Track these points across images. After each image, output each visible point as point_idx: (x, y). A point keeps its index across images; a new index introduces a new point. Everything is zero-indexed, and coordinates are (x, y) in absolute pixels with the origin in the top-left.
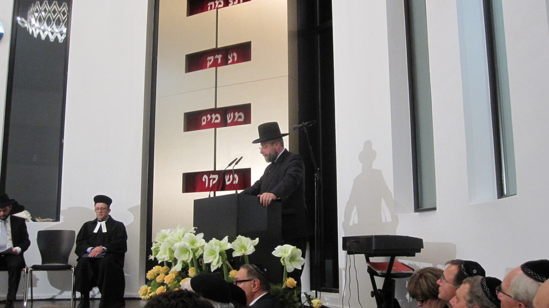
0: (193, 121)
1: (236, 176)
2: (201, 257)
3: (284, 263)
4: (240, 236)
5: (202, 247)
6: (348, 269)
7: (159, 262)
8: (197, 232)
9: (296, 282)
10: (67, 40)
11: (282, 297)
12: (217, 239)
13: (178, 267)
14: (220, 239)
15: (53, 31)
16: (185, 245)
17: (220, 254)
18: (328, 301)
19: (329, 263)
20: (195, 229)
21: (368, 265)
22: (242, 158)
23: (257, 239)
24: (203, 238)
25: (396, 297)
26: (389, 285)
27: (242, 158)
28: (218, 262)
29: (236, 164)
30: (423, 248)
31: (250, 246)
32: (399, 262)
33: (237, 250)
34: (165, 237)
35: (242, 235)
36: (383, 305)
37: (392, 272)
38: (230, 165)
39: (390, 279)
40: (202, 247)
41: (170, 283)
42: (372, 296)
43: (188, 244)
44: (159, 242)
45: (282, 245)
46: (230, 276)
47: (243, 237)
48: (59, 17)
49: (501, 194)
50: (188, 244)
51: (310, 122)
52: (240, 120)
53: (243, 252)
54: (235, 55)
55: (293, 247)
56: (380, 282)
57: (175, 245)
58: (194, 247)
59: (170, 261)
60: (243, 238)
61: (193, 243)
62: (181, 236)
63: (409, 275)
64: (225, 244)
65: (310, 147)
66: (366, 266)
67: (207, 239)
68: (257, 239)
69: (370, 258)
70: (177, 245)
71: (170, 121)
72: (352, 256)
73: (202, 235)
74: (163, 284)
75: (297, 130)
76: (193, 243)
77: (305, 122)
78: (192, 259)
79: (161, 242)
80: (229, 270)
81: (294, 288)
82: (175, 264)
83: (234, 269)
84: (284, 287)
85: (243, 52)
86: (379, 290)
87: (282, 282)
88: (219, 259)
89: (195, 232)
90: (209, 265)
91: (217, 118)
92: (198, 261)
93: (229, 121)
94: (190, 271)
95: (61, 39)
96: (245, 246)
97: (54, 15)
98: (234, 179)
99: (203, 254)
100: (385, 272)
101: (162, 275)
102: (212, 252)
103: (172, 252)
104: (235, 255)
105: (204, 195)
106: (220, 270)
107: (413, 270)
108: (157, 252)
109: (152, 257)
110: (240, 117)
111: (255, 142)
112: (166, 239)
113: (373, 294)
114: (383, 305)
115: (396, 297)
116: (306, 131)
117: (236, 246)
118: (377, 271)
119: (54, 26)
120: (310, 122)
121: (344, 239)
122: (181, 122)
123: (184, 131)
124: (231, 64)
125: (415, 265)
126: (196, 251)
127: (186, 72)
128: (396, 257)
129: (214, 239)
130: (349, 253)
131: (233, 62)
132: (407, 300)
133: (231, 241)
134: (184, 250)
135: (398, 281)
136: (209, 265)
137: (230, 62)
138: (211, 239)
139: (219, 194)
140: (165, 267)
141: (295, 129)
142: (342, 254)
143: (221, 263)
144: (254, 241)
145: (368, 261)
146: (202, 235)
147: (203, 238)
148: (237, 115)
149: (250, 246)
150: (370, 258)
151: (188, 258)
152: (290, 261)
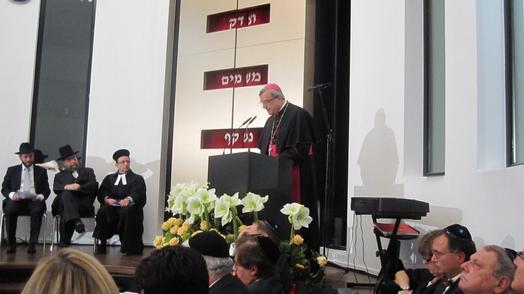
0: (213, 80)
1: (251, 134)
2: (213, 211)
3: (292, 221)
5: (214, 202)
6: (355, 228)
7: (174, 214)
8: (210, 187)
9: (303, 240)
11: (289, 253)
13: (191, 221)
14: (231, 195)
16: (197, 200)
18: (335, 258)
19: (338, 221)
20: (208, 185)
21: (375, 225)
22: (256, 117)
23: (267, 197)
24: (215, 194)
25: (401, 257)
26: (394, 246)
27: (256, 117)
28: (229, 217)
29: (250, 123)
30: (428, 212)
31: (260, 203)
32: (405, 224)
34: (180, 190)
35: (252, 192)
36: (388, 266)
37: (398, 234)
38: (244, 124)
39: (395, 240)
40: (214, 202)
41: (182, 235)
42: (377, 256)
43: (200, 199)
44: (174, 196)
45: (291, 203)
47: (253, 194)
49: (510, 162)
50: (200, 199)
51: (324, 84)
52: (256, 80)
53: (253, 208)
54: (254, 16)
55: (301, 206)
56: (385, 243)
57: (188, 199)
58: (206, 202)
59: (184, 214)
60: (253, 194)
61: (205, 198)
62: (194, 192)
63: (415, 237)
64: (235, 200)
65: (324, 109)
66: (372, 226)
67: (219, 194)
68: (267, 197)
69: (377, 220)
70: (190, 199)
71: (190, 79)
72: (359, 216)
73: (214, 190)
74: (176, 235)
75: (312, 92)
76: (205, 198)
77: (320, 84)
78: (204, 213)
79: (175, 196)
80: (239, 225)
81: (301, 245)
82: (189, 216)
83: (244, 224)
84: (291, 243)
85: (263, 13)
86: (385, 250)
87: (288, 239)
88: (229, 214)
89: (208, 187)
90: (220, 219)
92: (210, 216)
93: (247, 81)
94: (201, 225)
96: (255, 202)
98: (250, 137)
99: (214, 209)
100: (390, 233)
101: (176, 227)
102: (224, 207)
103: (185, 205)
104: (245, 210)
105: (218, 152)
106: (230, 224)
107: (419, 233)
108: (172, 204)
109: (168, 209)
110: (257, 77)
111: (17, 153)
112: (180, 193)
113: (378, 254)
114: (388, 266)
115: (400, 258)
116: (320, 93)
117: (246, 202)
118: (383, 233)
120: (324, 84)
121: (353, 199)
122: (201, 81)
123: (204, 90)
124: (250, 25)
125: (421, 227)
126: (208, 206)
127: (207, 32)
128: (402, 220)
129: (225, 195)
130: (357, 213)
131: (252, 24)
132: (412, 261)
133: (241, 197)
134: (197, 204)
135: (403, 243)
136: (220, 219)
137: (250, 23)
138: (223, 195)
139: (235, 151)
140: (180, 219)
141: (309, 90)
142: (350, 213)
143: (231, 218)
144: (264, 198)
145: (375, 221)
146: (214, 190)
147: (215, 194)
148: (254, 75)
149: (260, 203)
150: (377, 220)
151: (200, 212)
152: (298, 219)
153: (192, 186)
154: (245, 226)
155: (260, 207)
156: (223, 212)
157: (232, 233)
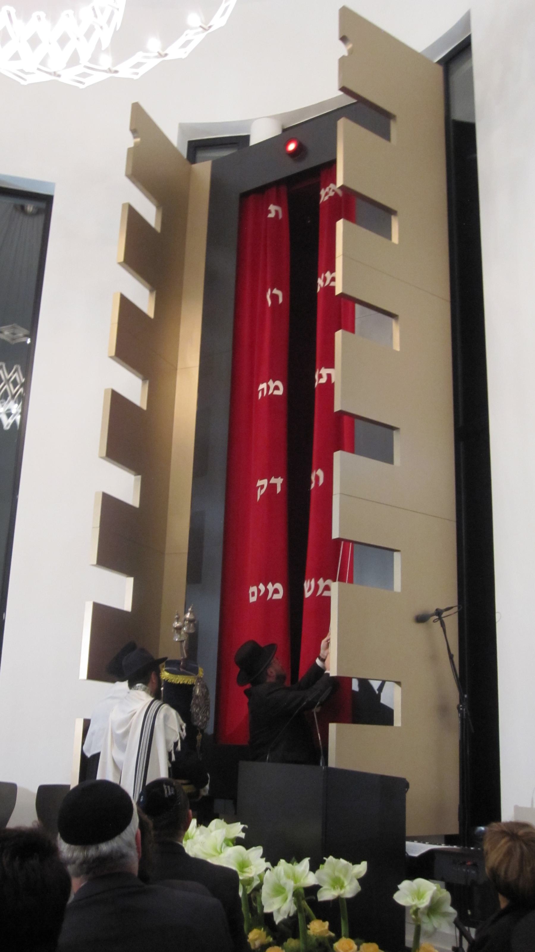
12: (288, 861)
17: (296, 894)
20: (244, 830)
23: (364, 864)
24: (262, 857)
33: (325, 887)
40: (261, 877)
46: (310, 932)
48: (6, 390)
62: (219, 850)
64: (302, 873)
68: (364, 864)
73: (258, 851)
80: (308, 920)
83: (319, 917)
91: (276, 591)
96: (342, 878)
117: (325, 878)
133: (314, 868)
146: (258, 851)
147: (262, 857)
153: (213, 834)
154: (321, 921)
155: (350, 889)
156: (279, 899)
157: (295, 936)
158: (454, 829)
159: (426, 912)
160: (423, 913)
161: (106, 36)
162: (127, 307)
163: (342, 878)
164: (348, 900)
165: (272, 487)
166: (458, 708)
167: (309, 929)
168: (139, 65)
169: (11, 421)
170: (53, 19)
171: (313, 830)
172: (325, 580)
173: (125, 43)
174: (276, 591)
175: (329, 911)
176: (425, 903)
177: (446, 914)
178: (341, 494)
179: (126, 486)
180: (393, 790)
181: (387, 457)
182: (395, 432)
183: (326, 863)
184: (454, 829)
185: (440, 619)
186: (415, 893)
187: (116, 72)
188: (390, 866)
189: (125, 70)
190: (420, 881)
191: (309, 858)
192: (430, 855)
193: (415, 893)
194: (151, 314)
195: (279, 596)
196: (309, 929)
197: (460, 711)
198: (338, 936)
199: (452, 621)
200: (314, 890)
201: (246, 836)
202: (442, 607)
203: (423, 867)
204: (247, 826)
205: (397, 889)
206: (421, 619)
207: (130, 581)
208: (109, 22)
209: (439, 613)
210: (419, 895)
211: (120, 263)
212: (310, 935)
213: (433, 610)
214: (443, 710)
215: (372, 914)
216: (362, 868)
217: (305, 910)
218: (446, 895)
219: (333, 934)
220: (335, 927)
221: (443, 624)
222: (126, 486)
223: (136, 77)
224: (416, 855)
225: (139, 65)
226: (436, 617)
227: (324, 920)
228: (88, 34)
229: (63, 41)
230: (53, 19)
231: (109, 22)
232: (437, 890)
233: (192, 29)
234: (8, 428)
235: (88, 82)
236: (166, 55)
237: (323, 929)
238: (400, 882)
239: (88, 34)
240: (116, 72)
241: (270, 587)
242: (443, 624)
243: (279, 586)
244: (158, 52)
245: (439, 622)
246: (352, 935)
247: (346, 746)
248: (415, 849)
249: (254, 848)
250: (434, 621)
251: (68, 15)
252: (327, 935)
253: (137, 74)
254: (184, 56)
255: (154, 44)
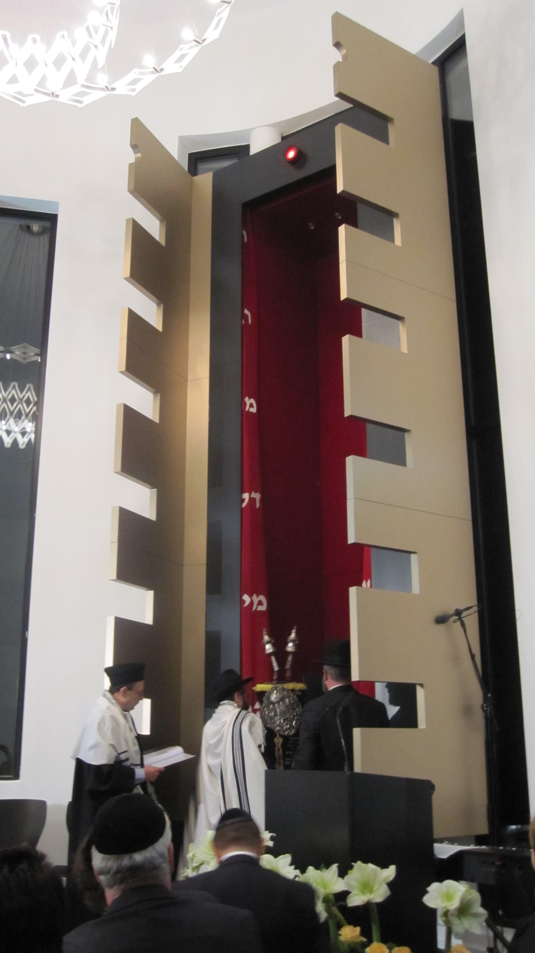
4: (359, 863)
10: (33, 449)
12: (317, 867)
15: (9, 429)
33: (354, 892)
46: (342, 938)
48: (20, 410)
73: (287, 858)
80: (339, 926)
83: (350, 923)
95: (22, 442)
96: (370, 883)
97: (12, 405)
117: (354, 883)
119: (12, 421)
133: (342, 873)
147: (291, 864)
155: (380, 894)
158: (483, 828)
159: (456, 913)
160: (453, 915)
161: (101, 55)
162: (135, 322)
163: (370, 883)
164: (378, 904)
165: (252, 501)
166: (482, 707)
167: (340, 935)
168: (135, 81)
169: (26, 440)
170: (49, 42)
171: (340, 836)
172: (257, 596)
173: (120, 60)
174: (260, 603)
175: (359, 916)
176: (454, 905)
177: (476, 915)
178: (355, 498)
179: (142, 500)
180: (419, 792)
181: (400, 459)
182: (406, 434)
183: (355, 869)
184: (483, 828)
185: (460, 619)
186: (444, 896)
187: (113, 89)
188: (419, 868)
189: (122, 87)
190: (449, 883)
191: (337, 865)
192: (458, 857)
193: (444, 896)
194: (160, 329)
195: (263, 608)
196: (340, 935)
197: (484, 711)
198: (370, 941)
199: (472, 621)
200: (343, 895)
201: (274, 844)
202: (462, 607)
203: (452, 869)
204: (274, 835)
205: (426, 892)
206: (441, 620)
207: (150, 595)
208: (103, 41)
209: (458, 613)
210: (449, 897)
211: (126, 279)
212: (341, 941)
213: (452, 611)
214: (467, 710)
215: (403, 917)
216: (391, 872)
217: (336, 917)
218: (475, 896)
219: (364, 940)
220: (366, 933)
221: (463, 625)
222: (142, 500)
223: (133, 94)
224: (445, 856)
225: (135, 81)
226: (456, 617)
227: (355, 926)
228: (84, 55)
229: (59, 62)
230: (49, 42)
231: (103, 41)
232: (466, 891)
233: (185, 43)
234: (23, 447)
235: (87, 100)
236: (162, 70)
237: (354, 935)
238: (429, 885)
239: (84, 55)
240: (113, 89)
241: (256, 599)
242: (463, 625)
243: (262, 598)
244: (154, 68)
245: (458, 623)
246: (384, 940)
247: (371, 751)
248: (444, 851)
249: (282, 856)
250: (454, 622)
251: (63, 35)
252: (358, 940)
253: (134, 90)
254: (180, 70)
255: (149, 60)
